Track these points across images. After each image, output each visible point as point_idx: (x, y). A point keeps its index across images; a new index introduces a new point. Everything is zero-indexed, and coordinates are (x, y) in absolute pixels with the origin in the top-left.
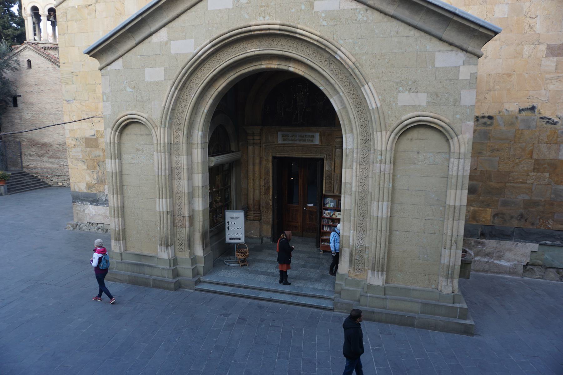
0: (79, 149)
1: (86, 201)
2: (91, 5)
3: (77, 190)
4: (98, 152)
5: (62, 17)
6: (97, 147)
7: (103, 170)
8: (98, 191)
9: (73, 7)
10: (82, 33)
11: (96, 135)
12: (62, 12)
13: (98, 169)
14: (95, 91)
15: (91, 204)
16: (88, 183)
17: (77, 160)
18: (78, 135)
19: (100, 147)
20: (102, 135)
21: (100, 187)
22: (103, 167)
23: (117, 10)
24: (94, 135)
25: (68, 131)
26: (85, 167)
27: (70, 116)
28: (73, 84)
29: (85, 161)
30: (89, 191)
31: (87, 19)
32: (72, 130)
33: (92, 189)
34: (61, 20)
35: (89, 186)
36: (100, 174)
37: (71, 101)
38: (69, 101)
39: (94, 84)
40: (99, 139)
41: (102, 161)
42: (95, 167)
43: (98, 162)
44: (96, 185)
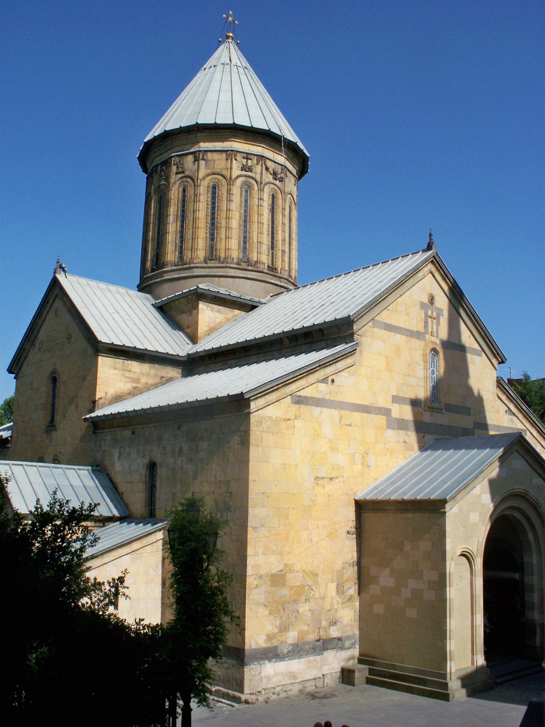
0: (262, 590)
1: (262, 659)
2: (290, 420)
3: (253, 647)
4: (284, 592)
5: (256, 426)
6: (283, 585)
7: (287, 613)
8: (279, 642)
9: (270, 418)
10: (278, 448)
11: (284, 570)
12: (257, 420)
13: (282, 613)
14: (287, 516)
15: (270, 661)
16: (269, 633)
17: (257, 604)
18: (262, 572)
19: (287, 584)
20: (291, 570)
21: (283, 635)
22: (288, 609)
23: (315, 431)
24: (282, 571)
25: (251, 566)
26: (267, 612)
27: (255, 547)
28: (263, 507)
29: (268, 605)
30: (269, 645)
31: (285, 434)
32: (256, 565)
33: (272, 641)
34: (255, 429)
35: (270, 638)
36: (284, 618)
37: (258, 528)
38: (256, 528)
39: (287, 509)
40: (287, 574)
41: (288, 601)
42: (279, 611)
43: (283, 604)
44: (279, 634)
